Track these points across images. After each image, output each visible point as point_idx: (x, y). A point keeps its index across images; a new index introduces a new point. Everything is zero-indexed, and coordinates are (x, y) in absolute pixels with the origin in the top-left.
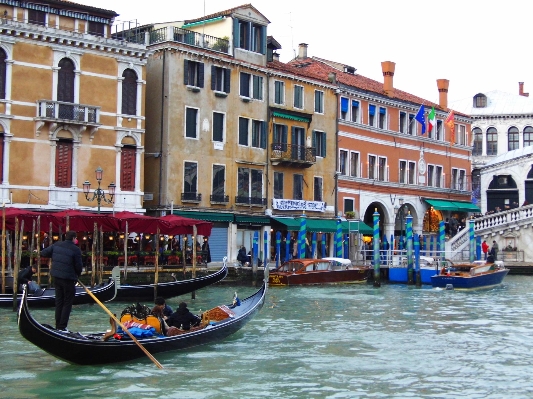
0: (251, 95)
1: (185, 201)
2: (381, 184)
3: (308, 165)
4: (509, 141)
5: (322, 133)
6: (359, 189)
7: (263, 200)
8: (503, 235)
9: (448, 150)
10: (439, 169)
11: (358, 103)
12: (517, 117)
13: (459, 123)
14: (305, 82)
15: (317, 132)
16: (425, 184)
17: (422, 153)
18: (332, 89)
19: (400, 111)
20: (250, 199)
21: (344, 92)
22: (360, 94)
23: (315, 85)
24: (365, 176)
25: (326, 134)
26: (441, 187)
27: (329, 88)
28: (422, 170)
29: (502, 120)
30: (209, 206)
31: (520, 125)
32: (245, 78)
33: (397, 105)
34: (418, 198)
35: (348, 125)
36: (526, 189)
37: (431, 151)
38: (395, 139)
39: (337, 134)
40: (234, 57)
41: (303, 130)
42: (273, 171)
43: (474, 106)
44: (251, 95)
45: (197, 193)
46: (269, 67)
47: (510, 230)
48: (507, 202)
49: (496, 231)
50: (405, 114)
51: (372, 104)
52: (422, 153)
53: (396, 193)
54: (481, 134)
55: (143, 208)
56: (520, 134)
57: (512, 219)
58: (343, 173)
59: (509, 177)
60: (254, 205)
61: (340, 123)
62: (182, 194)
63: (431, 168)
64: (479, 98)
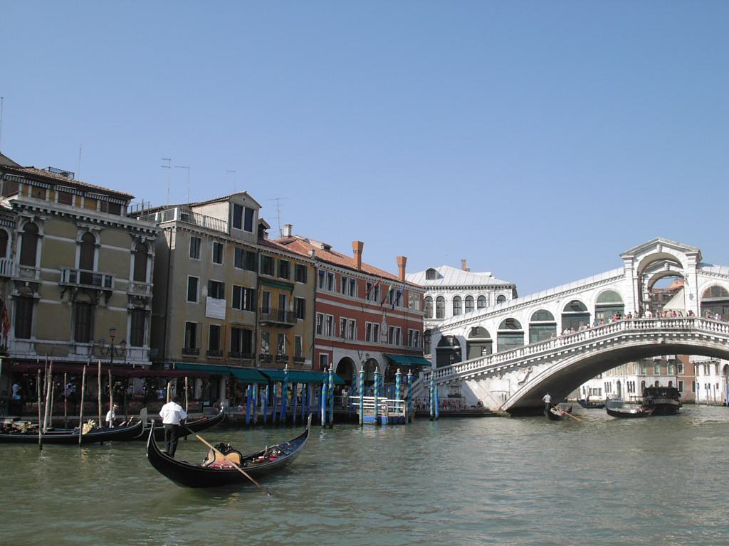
1: (185, 355)
6: (333, 346)
12: (460, 288)
15: (299, 300)
16: (387, 342)
20: (241, 354)
31: (463, 294)
38: (362, 305)
40: (230, 235)
55: (150, 361)
60: (245, 359)
64: (430, 272)
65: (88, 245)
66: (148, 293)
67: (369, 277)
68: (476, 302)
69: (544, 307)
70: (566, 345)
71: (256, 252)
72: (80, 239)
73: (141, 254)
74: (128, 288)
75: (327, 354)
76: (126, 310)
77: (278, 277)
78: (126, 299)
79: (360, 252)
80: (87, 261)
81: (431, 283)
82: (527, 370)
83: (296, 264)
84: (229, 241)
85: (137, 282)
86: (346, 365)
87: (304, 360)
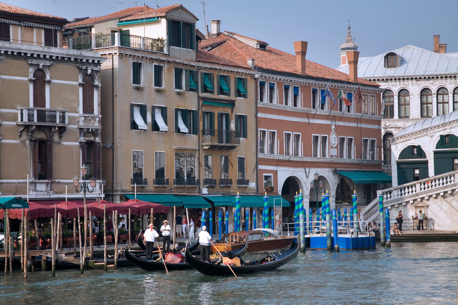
0: (184, 88)
2: (297, 159)
3: (233, 148)
5: (243, 116)
6: (277, 165)
7: (196, 181)
13: (369, 93)
14: (228, 71)
15: (240, 116)
16: (337, 156)
17: (333, 127)
18: (251, 74)
19: (312, 88)
20: (185, 181)
21: (261, 76)
22: (275, 76)
23: (237, 72)
24: (281, 153)
25: (246, 117)
26: (353, 158)
28: (334, 143)
29: (414, 81)
30: (153, 189)
31: (434, 86)
32: (178, 73)
33: (309, 83)
34: (330, 170)
35: (266, 106)
36: (435, 158)
37: (341, 124)
38: (308, 116)
39: (256, 115)
40: (169, 55)
41: (227, 115)
42: (204, 154)
43: (385, 66)
44: (184, 88)
45: (143, 178)
46: (198, 61)
47: (420, 200)
48: (417, 172)
50: (317, 90)
51: (286, 84)
52: (333, 127)
53: (310, 167)
54: (393, 96)
56: (433, 96)
57: (421, 189)
58: (262, 151)
59: (419, 148)
60: (189, 186)
61: (258, 105)
62: (131, 179)
63: (342, 140)
64: (390, 58)
65: (39, 82)
66: (97, 125)
67: (314, 82)
68: (451, 95)
71: (195, 70)
72: (31, 76)
73: (88, 86)
74: (79, 121)
75: (272, 175)
76: (77, 144)
77: (218, 94)
78: (78, 131)
79: (303, 53)
80: (39, 99)
81: (391, 72)
83: (235, 78)
84: (169, 62)
85: (86, 115)
86: (292, 185)
87: (247, 182)
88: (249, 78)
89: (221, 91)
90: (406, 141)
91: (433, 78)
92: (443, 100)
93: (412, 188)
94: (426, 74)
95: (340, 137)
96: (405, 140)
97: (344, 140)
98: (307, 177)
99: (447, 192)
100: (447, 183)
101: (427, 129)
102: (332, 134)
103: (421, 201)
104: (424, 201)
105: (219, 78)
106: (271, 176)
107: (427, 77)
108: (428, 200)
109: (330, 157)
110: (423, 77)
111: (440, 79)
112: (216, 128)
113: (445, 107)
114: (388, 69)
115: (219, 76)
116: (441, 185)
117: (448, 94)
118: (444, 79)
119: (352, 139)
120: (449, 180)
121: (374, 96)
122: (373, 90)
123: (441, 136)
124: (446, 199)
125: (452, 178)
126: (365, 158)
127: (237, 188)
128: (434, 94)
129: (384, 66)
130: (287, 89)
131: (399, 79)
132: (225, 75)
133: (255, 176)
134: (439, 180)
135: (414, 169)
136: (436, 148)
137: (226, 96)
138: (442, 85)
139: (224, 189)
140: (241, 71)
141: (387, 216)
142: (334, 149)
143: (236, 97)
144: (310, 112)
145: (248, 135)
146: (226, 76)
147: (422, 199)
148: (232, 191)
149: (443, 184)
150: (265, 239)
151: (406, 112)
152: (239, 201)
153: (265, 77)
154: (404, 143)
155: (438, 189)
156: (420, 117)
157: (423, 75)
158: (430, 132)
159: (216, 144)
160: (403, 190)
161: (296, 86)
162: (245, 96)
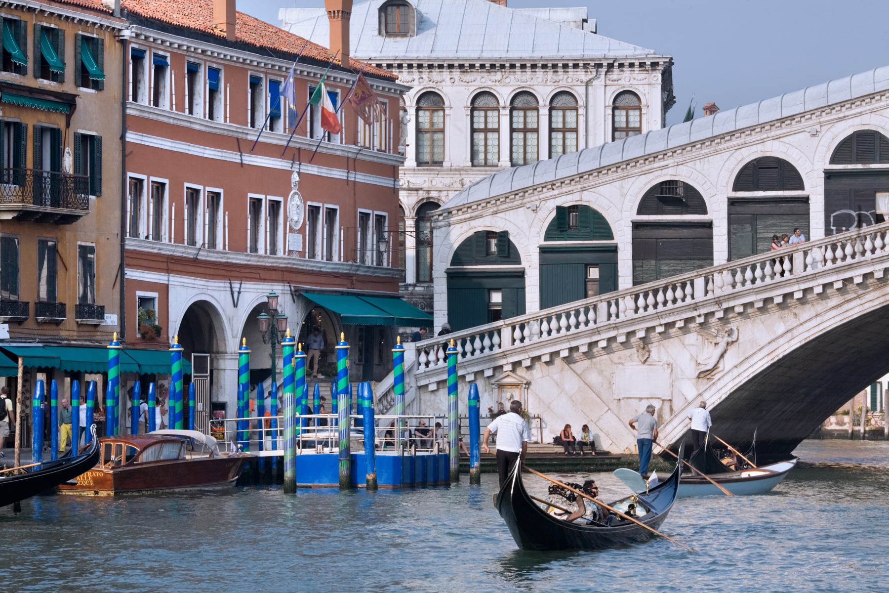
2: (213, 257)
3: (71, 219)
4: (473, 131)
5: (92, 137)
6: (168, 271)
8: (493, 381)
9: (351, 163)
10: (331, 213)
11: (166, 57)
14: (60, 16)
15: (85, 137)
16: (302, 254)
17: (295, 178)
18: (114, 29)
19: (249, 73)
21: (137, 35)
23: (81, 21)
24: (179, 239)
26: (336, 259)
27: (108, 27)
28: (296, 218)
29: (456, 74)
36: (544, 266)
37: (312, 170)
38: (239, 145)
41: (55, 134)
43: (380, 33)
47: (509, 367)
48: (496, 298)
49: (476, 369)
50: (260, 79)
51: (192, 60)
52: (295, 178)
53: (241, 279)
56: (502, 111)
57: (514, 340)
58: (135, 233)
59: (503, 237)
61: (129, 111)
63: (314, 212)
68: (544, 112)
69: (775, 149)
70: (839, 263)
75: (155, 295)
77: (36, 77)
82: (723, 341)
83: (76, 35)
86: (200, 322)
87: (100, 313)
88: (107, 38)
89: (44, 70)
90: (471, 219)
91: (503, 66)
92: (525, 123)
93: (491, 338)
94: (486, 55)
95: (309, 203)
96: (468, 216)
97: (318, 213)
98: (235, 305)
99: (577, 348)
100: (577, 326)
101: (525, 190)
102: (293, 197)
103: (513, 371)
104: (520, 371)
105: (38, 33)
106: (153, 299)
107: (488, 65)
108: (528, 368)
109: (286, 256)
110: (477, 65)
111: (518, 70)
112: (30, 164)
113: (529, 142)
114: (388, 39)
115: (38, 28)
116: (563, 331)
117: (537, 109)
118: (528, 70)
119: (335, 210)
120: (582, 318)
121: (385, 104)
122: (384, 88)
123: (560, 209)
124: (572, 366)
125: (591, 315)
126: (363, 260)
127: (75, 328)
128: (504, 108)
129: (377, 32)
130: (193, 72)
131: (420, 66)
132: (52, 26)
133: (117, 296)
134: (559, 317)
135: (490, 290)
136: (545, 240)
137: (53, 83)
138: (523, 85)
139: (45, 327)
140: (91, 18)
141: (473, 403)
142: (296, 235)
143: (77, 86)
144: (244, 136)
145: (103, 189)
146: (53, 29)
147: (516, 365)
148: (63, 334)
149: (568, 328)
150: (188, 457)
151: (436, 150)
152: (117, 358)
153: (146, 38)
154: (465, 226)
155: (555, 341)
156: (470, 164)
157: (478, 60)
158: (532, 199)
159: (32, 207)
160: (468, 343)
161: (215, 66)
162: (97, 86)
